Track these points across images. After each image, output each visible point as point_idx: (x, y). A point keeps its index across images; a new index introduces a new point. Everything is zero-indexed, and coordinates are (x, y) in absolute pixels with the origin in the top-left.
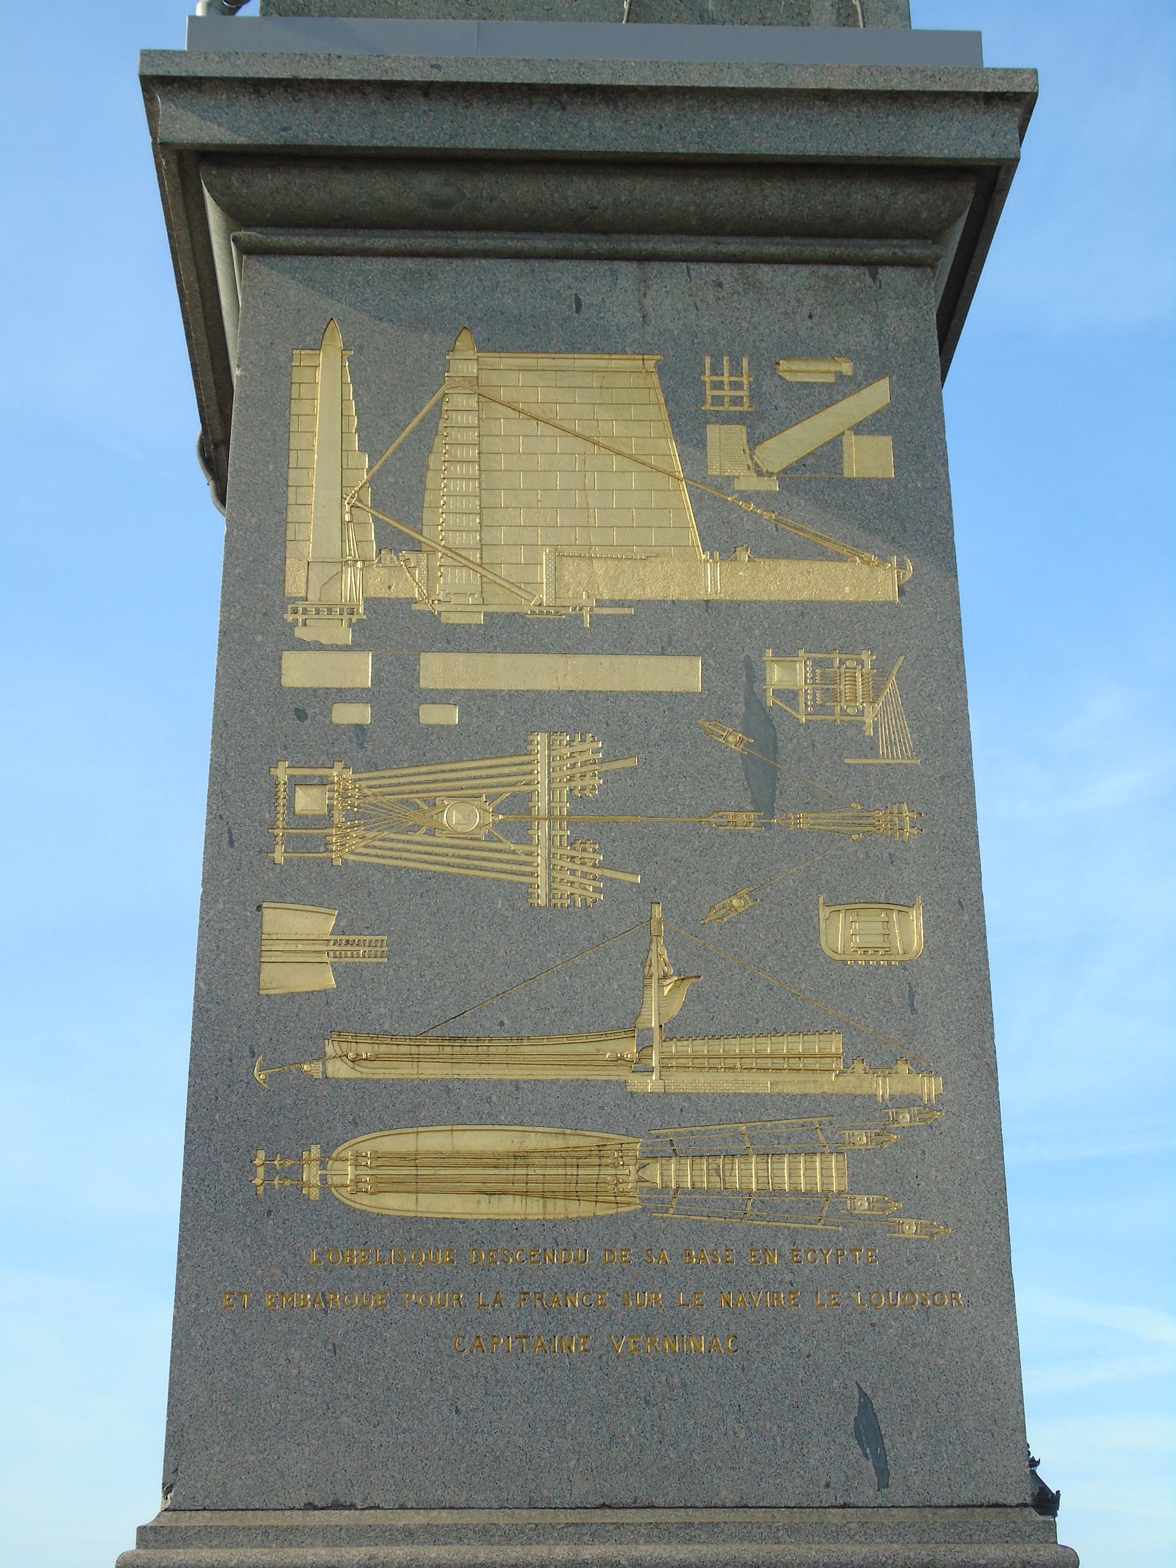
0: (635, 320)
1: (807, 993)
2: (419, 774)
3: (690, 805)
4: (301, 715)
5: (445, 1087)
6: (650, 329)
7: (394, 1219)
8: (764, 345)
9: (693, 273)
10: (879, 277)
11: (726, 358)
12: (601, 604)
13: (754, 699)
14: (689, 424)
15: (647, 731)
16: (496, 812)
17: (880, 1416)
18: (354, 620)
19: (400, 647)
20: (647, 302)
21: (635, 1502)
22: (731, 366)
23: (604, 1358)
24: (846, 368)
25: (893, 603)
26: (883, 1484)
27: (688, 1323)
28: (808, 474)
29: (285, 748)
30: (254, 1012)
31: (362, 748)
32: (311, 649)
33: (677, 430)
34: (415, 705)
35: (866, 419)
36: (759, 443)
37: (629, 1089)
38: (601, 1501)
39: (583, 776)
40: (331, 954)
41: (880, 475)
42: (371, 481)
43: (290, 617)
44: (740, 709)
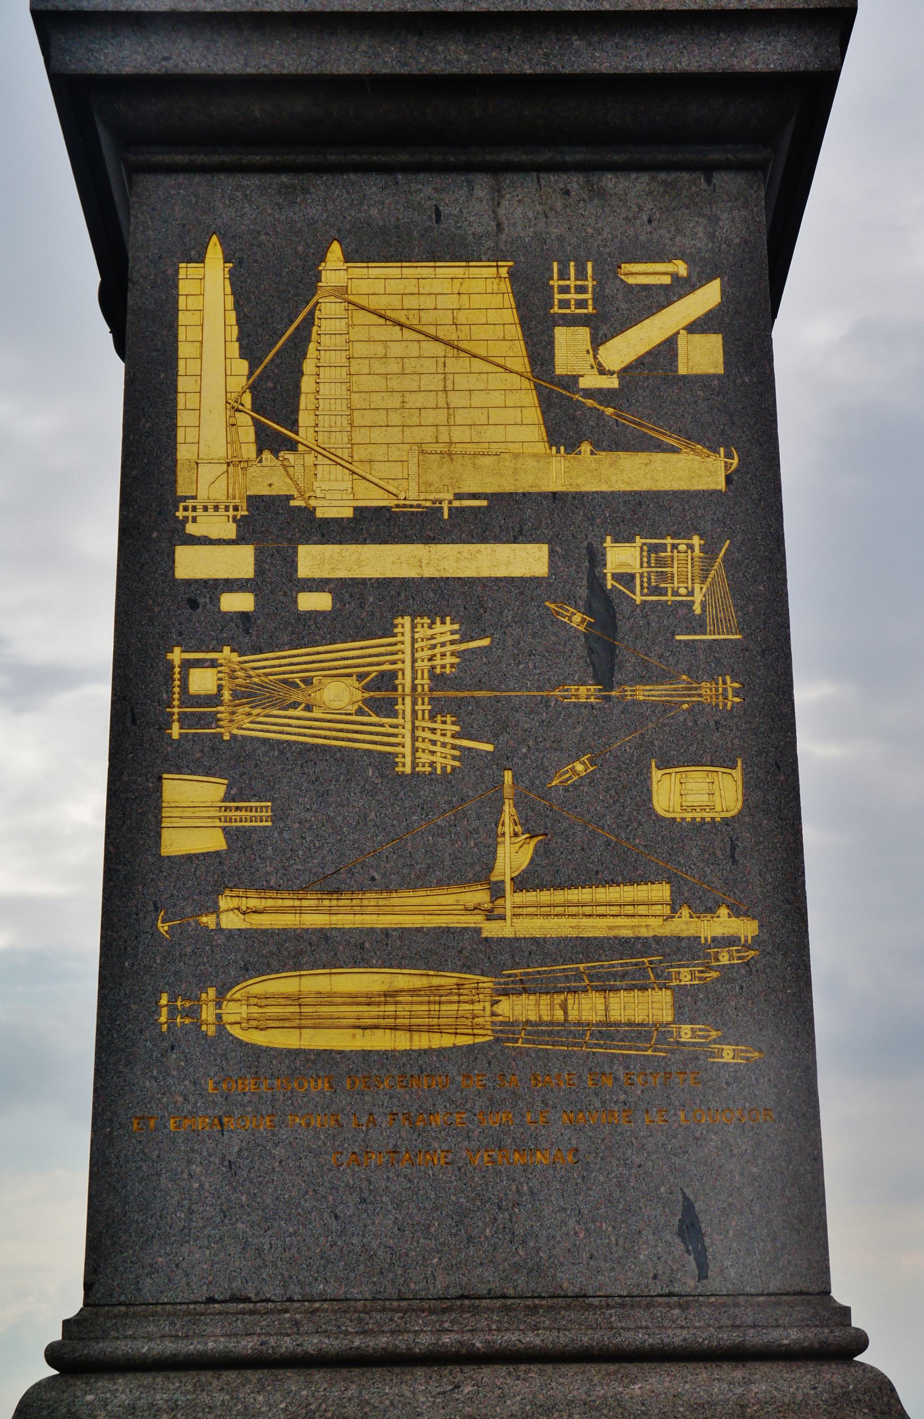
0: (490, 228)
1: (641, 848)
2: (298, 656)
3: (539, 680)
4: (193, 604)
5: (323, 935)
6: (503, 237)
7: (280, 1051)
8: (608, 250)
9: (543, 182)
10: (714, 181)
11: (572, 264)
12: (459, 496)
13: (596, 581)
14: (537, 326)
15: (501, 613)
16: (366, 688)
17: (702, 1217)
18: (238, 517)
19: (280, 540)
20: (501, 211)
21: (489, 1293)
22: (577, 271)
23: (463, 1170)
24: (681, 268)
25: (720, 491)
26: (703, 1275)
27: (535, 1139)
28: (646, 372)
29: (180, 634)
30: (157, 872)
31: (248, 633)
32: (201, 544)
33: (527, 333)
34: (294, 593)
35: (699, 318)
36: (602, 343)
37: (484, 935)
38: (461, 1292)
39: (443, 655)
40: (223, 819)
41: (711, 371)
42: (249, 388)
43: (180, 514)
44: (583, 592)
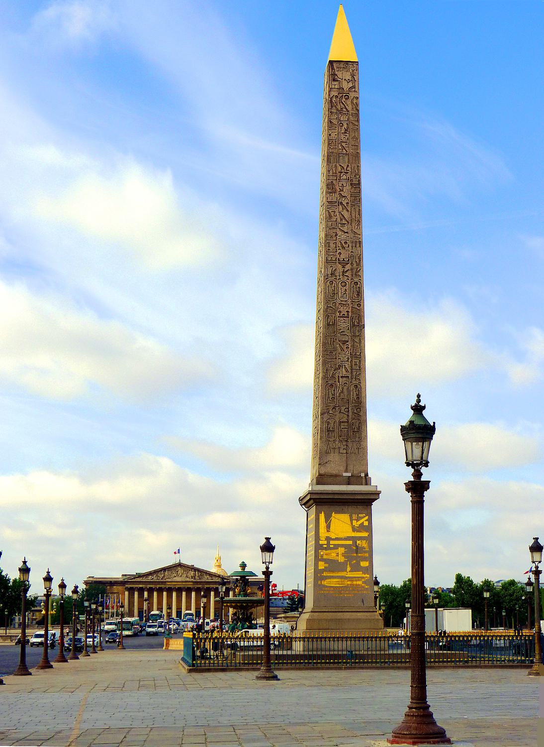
5: (333, 576)
13: (356, 545)
14: (351, 521)
